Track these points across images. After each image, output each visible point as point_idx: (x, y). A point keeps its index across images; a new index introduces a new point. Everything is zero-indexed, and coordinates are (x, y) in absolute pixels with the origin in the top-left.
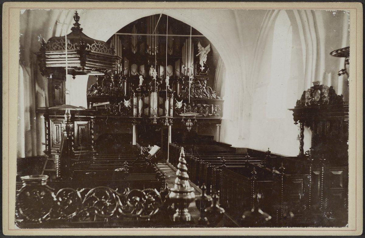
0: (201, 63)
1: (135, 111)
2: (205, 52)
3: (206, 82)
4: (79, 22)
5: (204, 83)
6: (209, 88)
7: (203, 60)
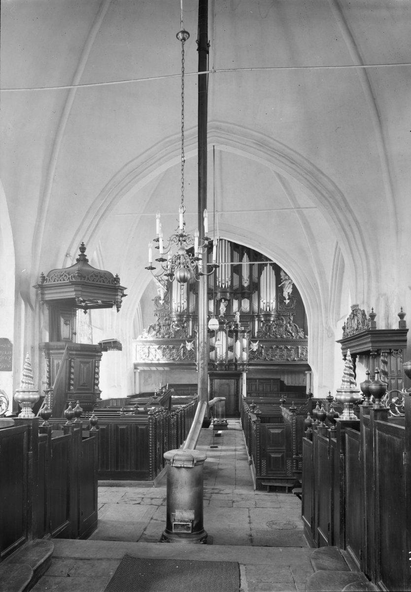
4: (85, 253)
5: (290, 319)
6: (294, 325)
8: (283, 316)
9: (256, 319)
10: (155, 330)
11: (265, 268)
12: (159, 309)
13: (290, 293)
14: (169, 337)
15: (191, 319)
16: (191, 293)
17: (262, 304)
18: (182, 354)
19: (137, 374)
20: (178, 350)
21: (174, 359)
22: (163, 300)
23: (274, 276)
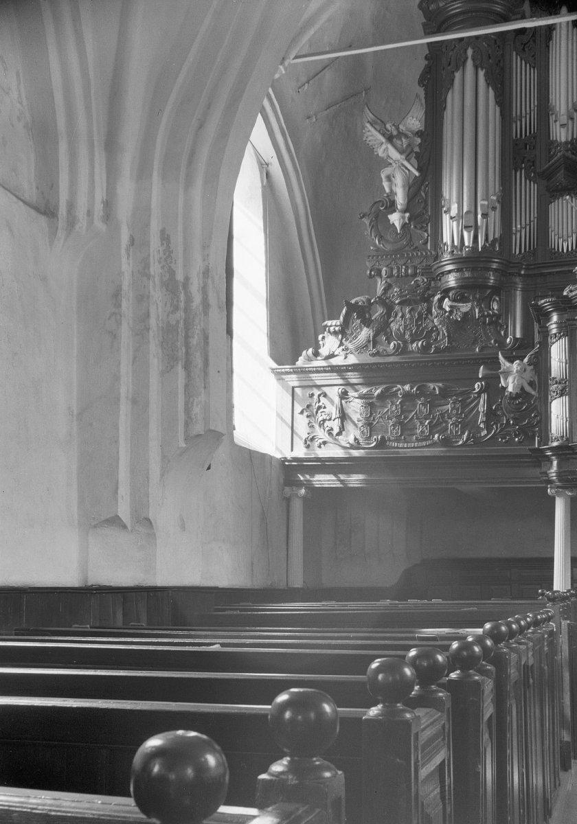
10: (367, 322)
12: (388, 247)
14: (425, 349)
15: (518, 280)
16: (520, 176)
18: (481, 418)
19: (297, 507)
20: (466, 402)
21: (446, 442)
22: (405, 211)
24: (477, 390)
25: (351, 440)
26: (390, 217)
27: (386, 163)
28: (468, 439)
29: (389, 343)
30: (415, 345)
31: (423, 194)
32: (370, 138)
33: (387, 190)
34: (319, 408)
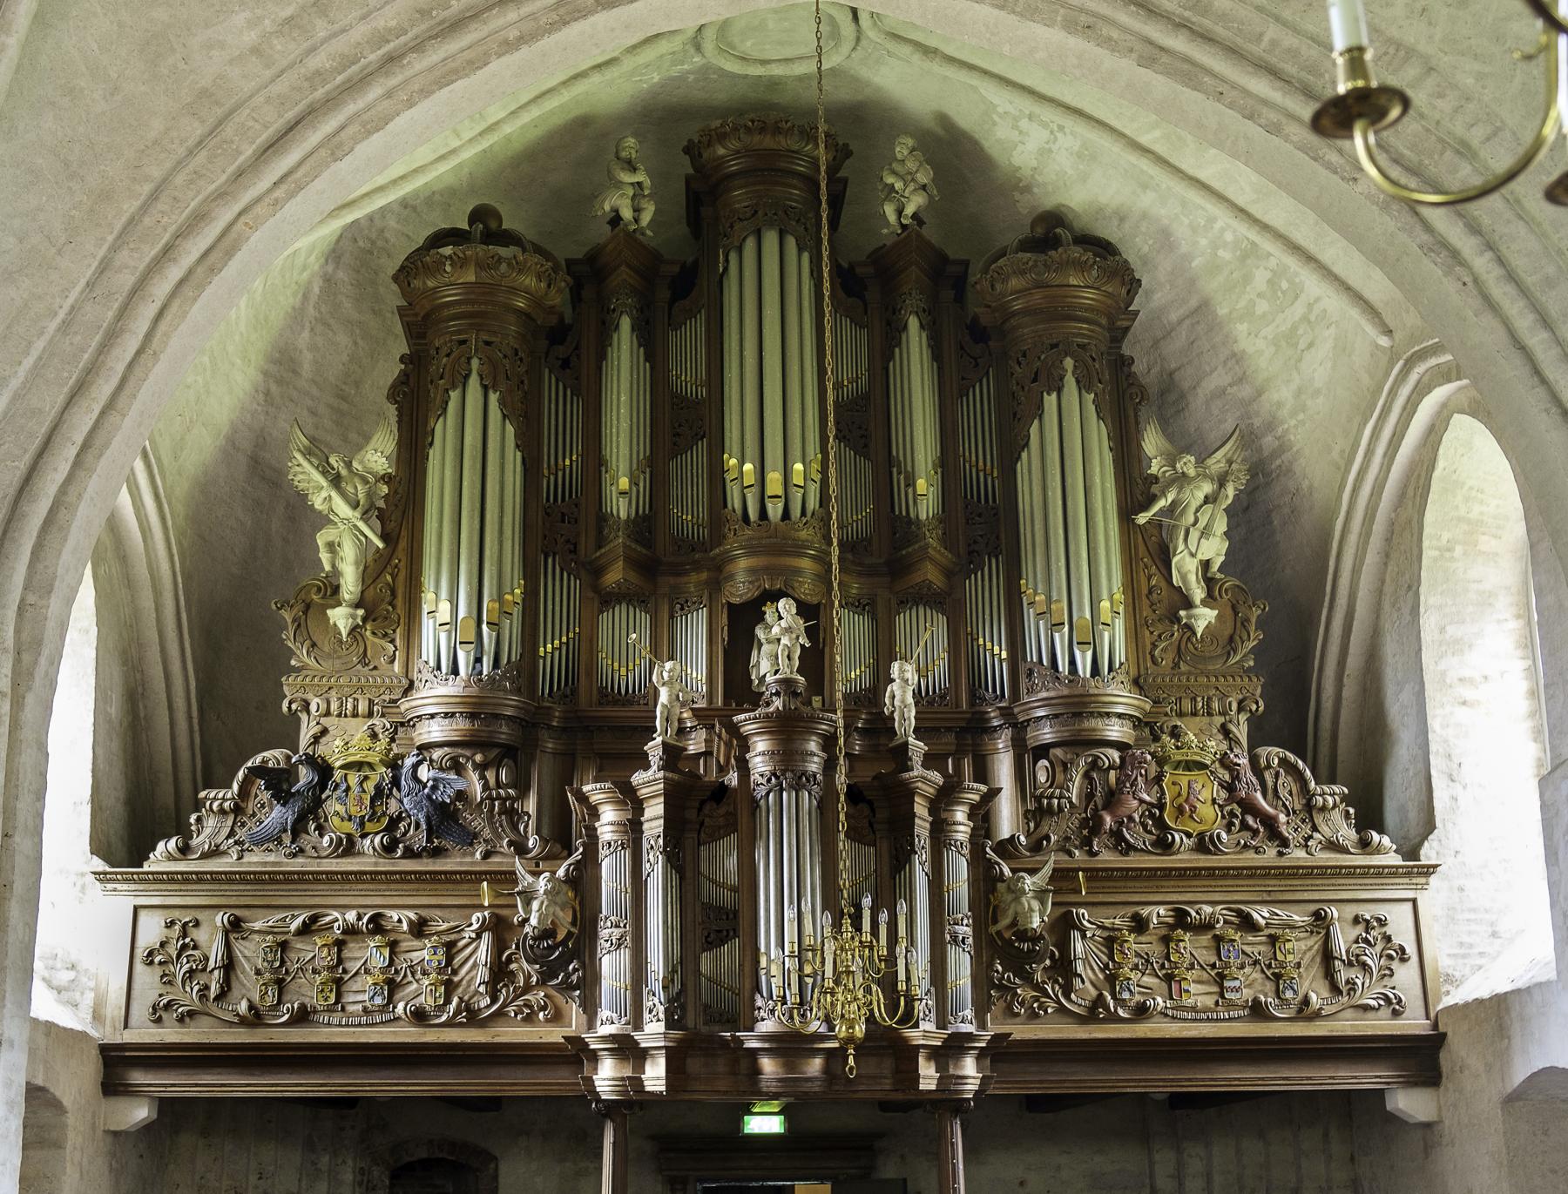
0: (1184, 577)
1: (612, 966)
2: (1208, 488)
3: (1244, 728)
6: (1284, 762)
7: (1202, 548)
8: (1181, 715)
9: (1003, 742)
11: (1050, 400)
13: (1215, 567)
17: (1035, 628)
18: (482, 974)
23: (1108, 457)
24: (475, 926)
25: (243, 1007)
26: (329, 612)
27: (324, 520)
28: (458, 1012)
29: (321, 836)
30: (367, 842)
31: (389, 578)
32: (301, 477)
33: (327, 567)
34: (184, 947)
